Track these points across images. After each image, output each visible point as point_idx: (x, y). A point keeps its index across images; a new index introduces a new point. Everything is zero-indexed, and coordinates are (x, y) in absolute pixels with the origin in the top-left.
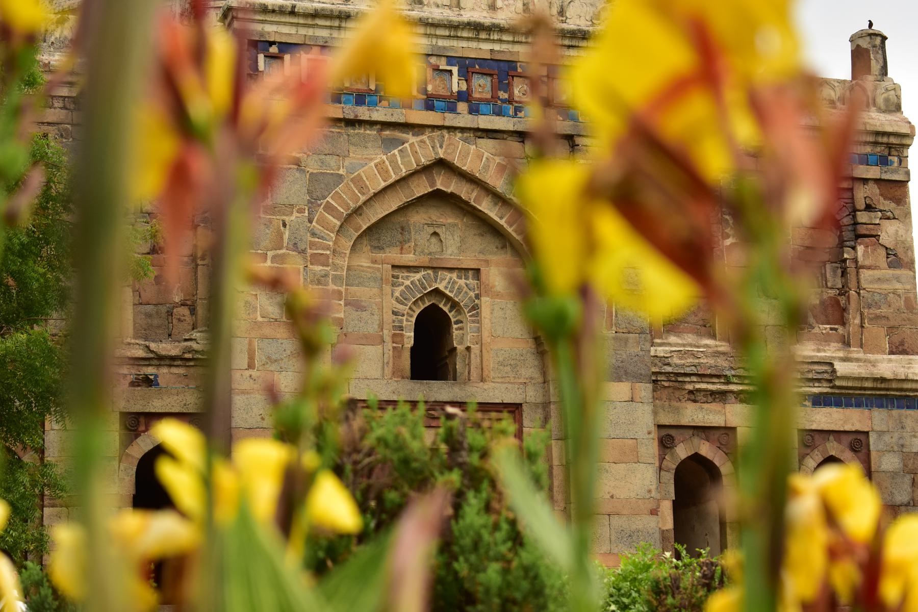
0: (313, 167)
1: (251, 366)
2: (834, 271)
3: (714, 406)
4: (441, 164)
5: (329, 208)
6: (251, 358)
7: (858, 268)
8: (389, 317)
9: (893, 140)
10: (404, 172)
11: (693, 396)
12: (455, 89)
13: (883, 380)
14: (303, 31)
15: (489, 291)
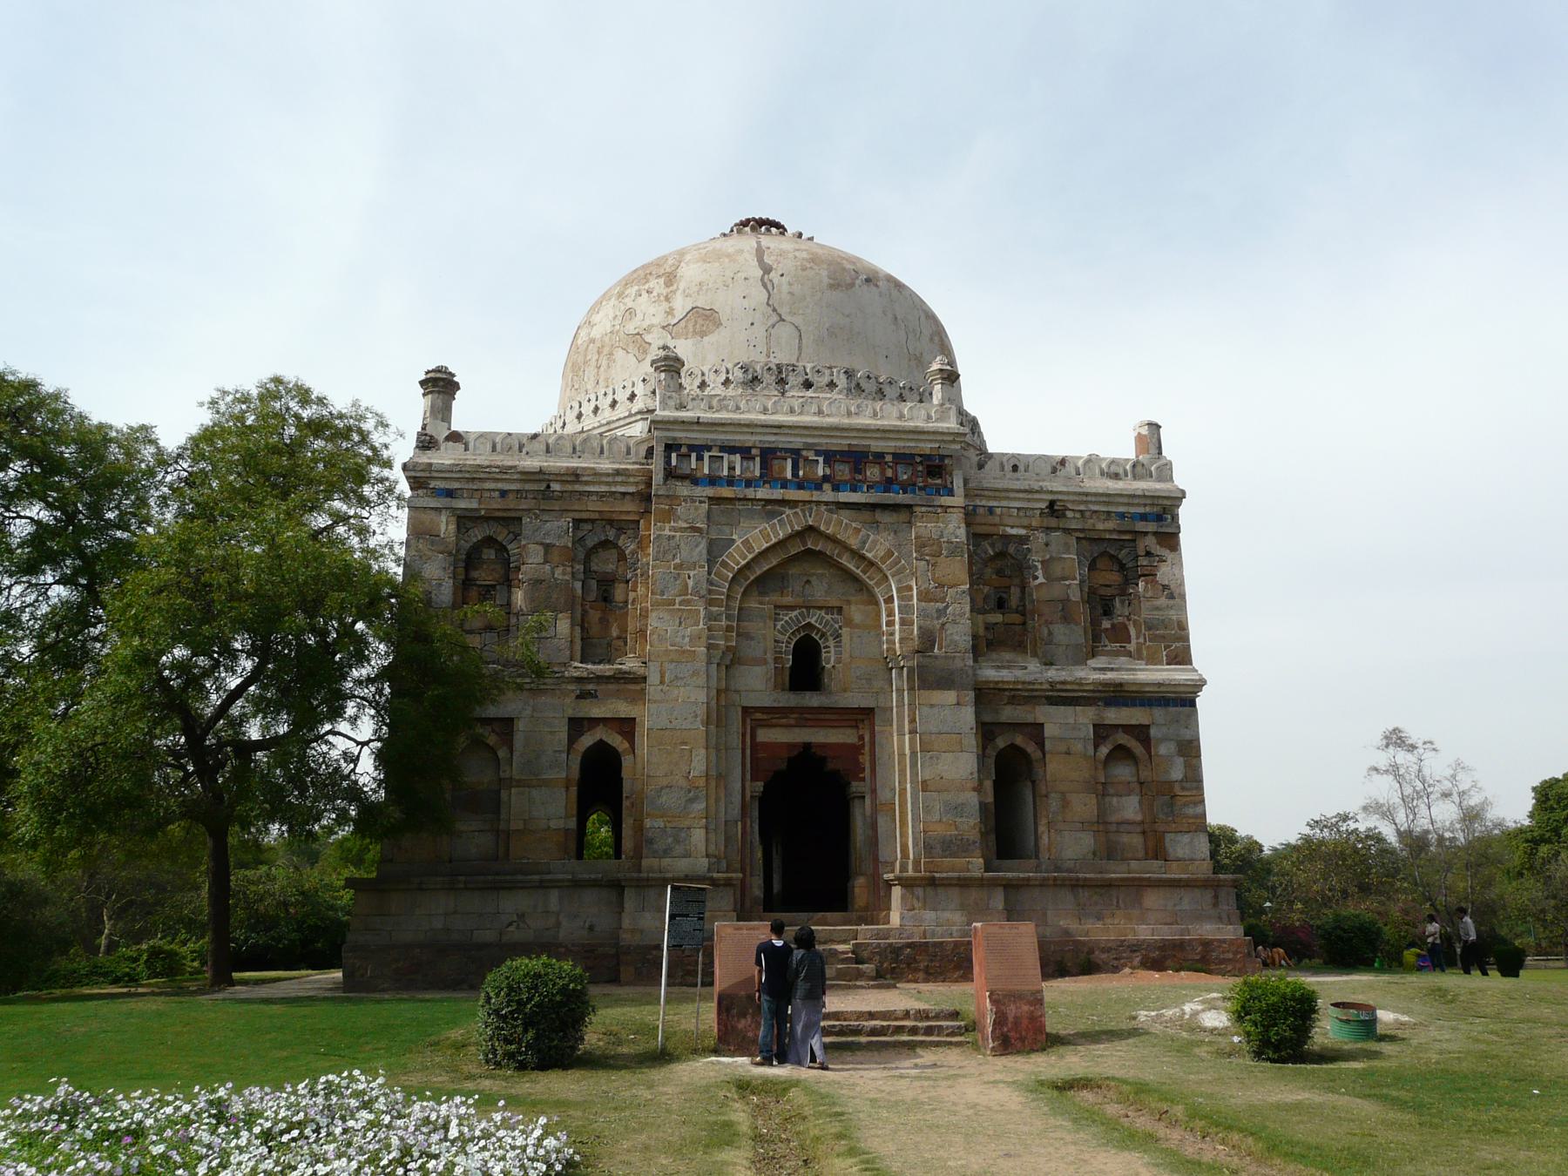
1: (662, 682)
2: (1122, 602)
3: (1028, 708)
4: (811, 529)
6: (662, 676)
8: (770, 644)
10: (781, 536)
12: (820, 473)
15: (849, 623)
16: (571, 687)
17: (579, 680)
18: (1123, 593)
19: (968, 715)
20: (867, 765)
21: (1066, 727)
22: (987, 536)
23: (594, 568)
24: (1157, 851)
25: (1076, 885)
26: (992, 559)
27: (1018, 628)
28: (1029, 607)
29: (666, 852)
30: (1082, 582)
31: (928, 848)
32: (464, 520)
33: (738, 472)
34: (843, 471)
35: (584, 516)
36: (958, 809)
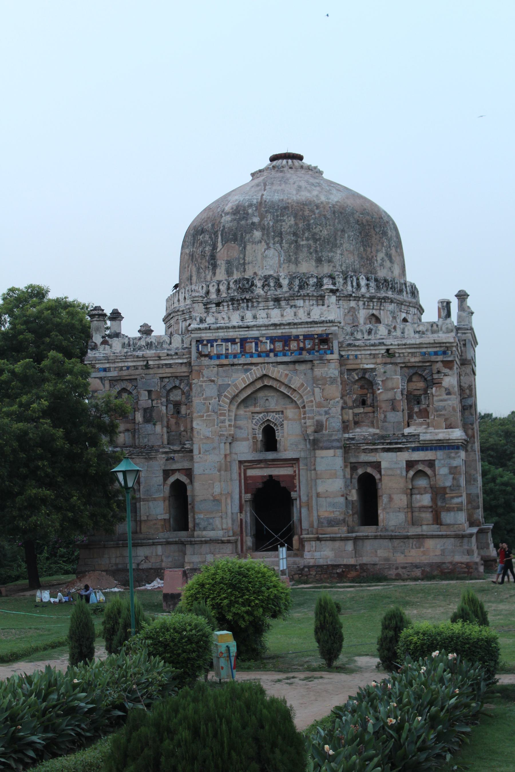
0: (220, 382)
1: (200, 453)
2: (425, 398)
3: (373, 454)
4: (265, 376)
5: (226, 396)
7: (433, 396)
8: (250, 431)
9: (448, 345)
10: (251, 380)
11: (365, 451)
12: (268, 348)
13: (440, 440)
14: (214, 335)
15: (286, 418)
16: (164, 456)
17: (166, 453)
18: (426, 393)
19: (339, 462)
20: (297, 484)
21: (392, 463)
23: (172, 399)
24: (437, 520)
26: (357, 381)
27: (371, 415)
28: (375, 404)
29: (205, 529)
33: (230, 351)
35: (165, 375)
36: (334, 505)
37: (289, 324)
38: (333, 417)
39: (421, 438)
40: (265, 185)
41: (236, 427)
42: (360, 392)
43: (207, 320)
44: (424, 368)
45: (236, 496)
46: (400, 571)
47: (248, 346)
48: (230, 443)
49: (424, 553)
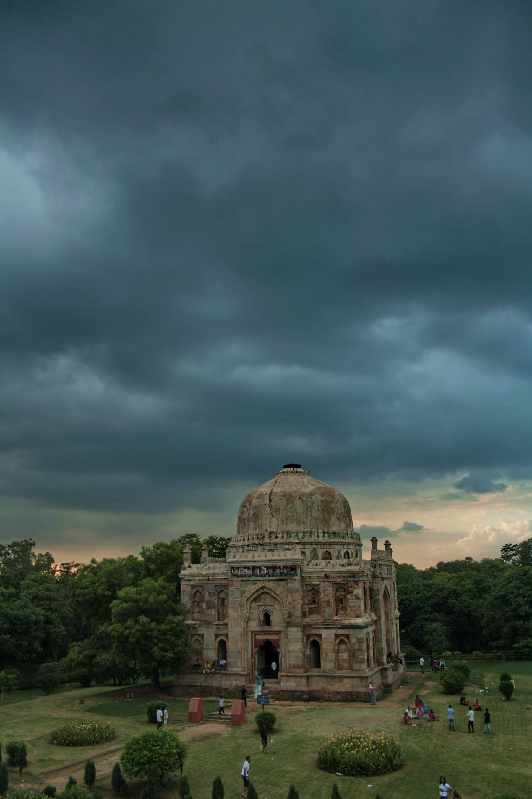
4: (263, 587)
8: (257, 615)
10: (257, 589)
15: (275, 609)
17: (216, 625)
18: (345, 598)
19: (300, 634)
22: (309, 584)
24: (351, 668)
25: (326, 677)
29: (233, 667)
30: (333, 596)
31: (290, 667)
32: (193, 586)
34: (271, 571)
37: (275, 560)
38: (297, 610)
39: (342, 622)
40: (276, 482)
41: (250, 613)
42: (312, 596)
43: (237, 556)
44: (344, 584)
45: (250, 650)
46: (330, 695)
47: (255, 571)
48: (247, 622)
49: (343, 686)
